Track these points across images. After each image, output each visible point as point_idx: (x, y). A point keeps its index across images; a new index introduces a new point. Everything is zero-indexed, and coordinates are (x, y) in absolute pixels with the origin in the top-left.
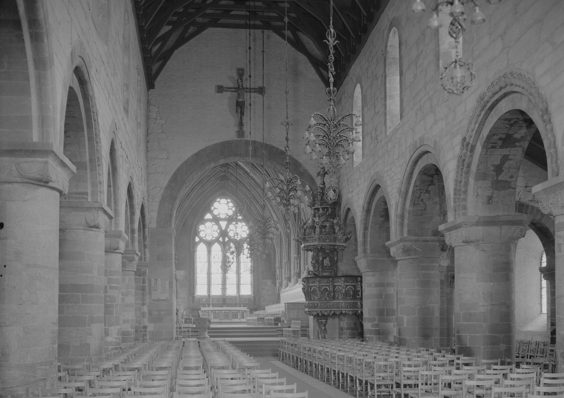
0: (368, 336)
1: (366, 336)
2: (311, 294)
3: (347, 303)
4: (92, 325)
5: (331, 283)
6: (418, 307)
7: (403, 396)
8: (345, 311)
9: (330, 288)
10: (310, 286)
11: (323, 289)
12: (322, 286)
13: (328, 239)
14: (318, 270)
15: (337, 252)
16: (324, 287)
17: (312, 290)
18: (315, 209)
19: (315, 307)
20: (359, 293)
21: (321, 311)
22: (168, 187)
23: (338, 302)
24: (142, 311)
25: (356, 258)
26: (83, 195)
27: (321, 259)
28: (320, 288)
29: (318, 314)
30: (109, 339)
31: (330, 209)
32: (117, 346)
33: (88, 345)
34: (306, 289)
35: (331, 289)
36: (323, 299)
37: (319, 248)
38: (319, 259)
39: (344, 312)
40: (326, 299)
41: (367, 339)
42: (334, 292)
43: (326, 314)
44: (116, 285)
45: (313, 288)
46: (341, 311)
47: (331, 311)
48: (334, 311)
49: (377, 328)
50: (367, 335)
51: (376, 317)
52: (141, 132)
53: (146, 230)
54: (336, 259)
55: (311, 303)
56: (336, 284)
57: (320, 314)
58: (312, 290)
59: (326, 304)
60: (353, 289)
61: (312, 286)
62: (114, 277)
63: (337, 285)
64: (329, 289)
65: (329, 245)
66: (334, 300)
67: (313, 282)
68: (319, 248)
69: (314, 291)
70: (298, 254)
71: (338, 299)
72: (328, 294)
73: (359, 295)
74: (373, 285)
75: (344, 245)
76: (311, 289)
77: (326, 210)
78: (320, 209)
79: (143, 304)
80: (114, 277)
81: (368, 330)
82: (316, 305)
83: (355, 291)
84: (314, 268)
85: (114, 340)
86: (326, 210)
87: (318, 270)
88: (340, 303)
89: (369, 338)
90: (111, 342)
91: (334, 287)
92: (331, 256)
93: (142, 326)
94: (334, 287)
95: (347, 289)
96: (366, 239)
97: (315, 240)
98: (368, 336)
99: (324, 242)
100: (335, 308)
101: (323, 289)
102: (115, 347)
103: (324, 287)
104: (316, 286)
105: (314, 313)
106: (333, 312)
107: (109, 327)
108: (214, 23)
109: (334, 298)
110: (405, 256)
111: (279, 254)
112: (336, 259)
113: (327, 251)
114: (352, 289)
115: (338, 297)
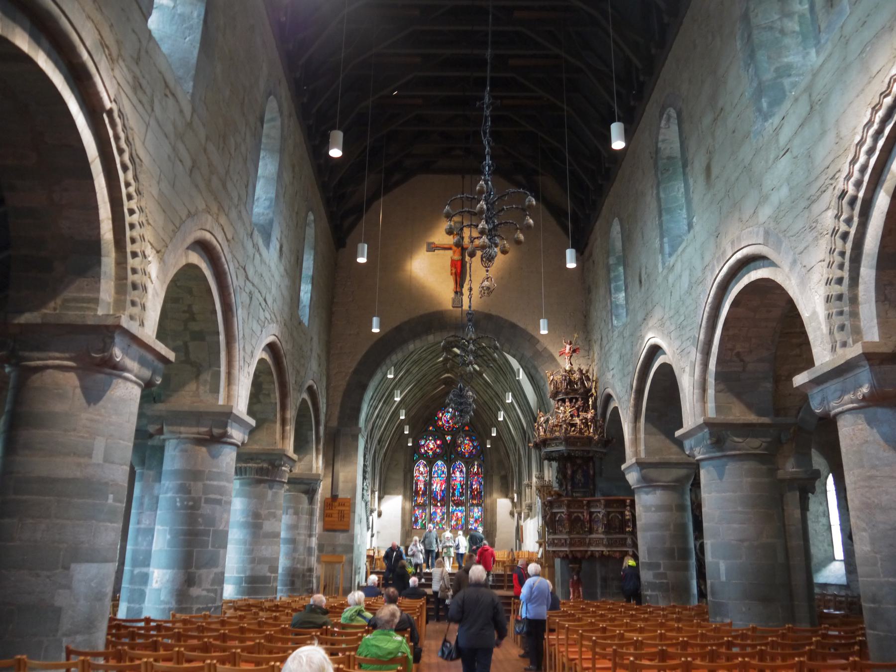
0: (649, 593)
1: (646, 593)
2: (557, 524)
3: (611, 539)
4: (73, 566)
5: (585, 507)
6: (746, 544)
8: (609, 551)
9: (584, 516)
10: (555, 513)
11: (573, 517)
12: (571, 512)
13: (580, 442)
14: (566, 488)
15: (594, 463)
17: (557, 518)
18: (558, 401)
19: (562, 545)
20: (629, 524)
21: (571, 551)
22: (356, 372)
24: (307, 546)
25: (623, 467)
26: (89, 302)
27: (569, 472)
28: (569, 515)
29: (567, 556)
30: (195, 591)
31: (580, 399)
32: (210, 605)
33: (58, 611)
34: (548, 517)
35: (585, 516)
37: (566, 455)
38: (567, 473)
39: (608, 553)
40: (578, 533)
41: (648, 598)
42: (591, 521)
43: (579, 555)
44: (219, 497)
45: (559, 515)
46: (602, 551)
47: (586, 551)
48: (592, 551)
49: (665, 581)
50: (647, 593)
51: (661, 562)
52: (279, 255)
53: (322, 428)
54: (591, 472)
55: (557, 539)
56: (593, 510)
57: (570, 556)
58: (557, 518)
61: (558, 513)
62: (215, 483)
63: (596, 512)
64: (582, 518)
65: (582, 450)
67: (560, 507)
68: (566, 455)
69: (561, 520)
70: (540, 471)
72: (581, 525)
73: (629, 527)
74: (653, 509)
75: (604, 451)
76: (555, 517)
77: (574, 401)
78: (567, 400)
79: (310, 536)
80: (215, 483)
81: (649, 583)
82: (563, 541)
84: (561, 485)
85: (204, 593)
86: (574, 401)
87: (566, 488)
89: (650, 596)
90: (198, 597)
91: (591, 514)
92: (585, 468)
93: (306, 567)
94: (591, 514)
95: (610, 517)
96: (638, 436)
97: (561, 443)
98: (649, 593)
101: (573, 517)
102: (205, 606)
103: (575, 514)
104: (563, 512)
105: (561, 554)
107: (195, 571)
108: (427, 167)
109: (591, 531)
110: (714, 452)
111: (517, 475)
112: (591, 472)
113: (579, 461)
114: (618, 517)
115: (597, 530)
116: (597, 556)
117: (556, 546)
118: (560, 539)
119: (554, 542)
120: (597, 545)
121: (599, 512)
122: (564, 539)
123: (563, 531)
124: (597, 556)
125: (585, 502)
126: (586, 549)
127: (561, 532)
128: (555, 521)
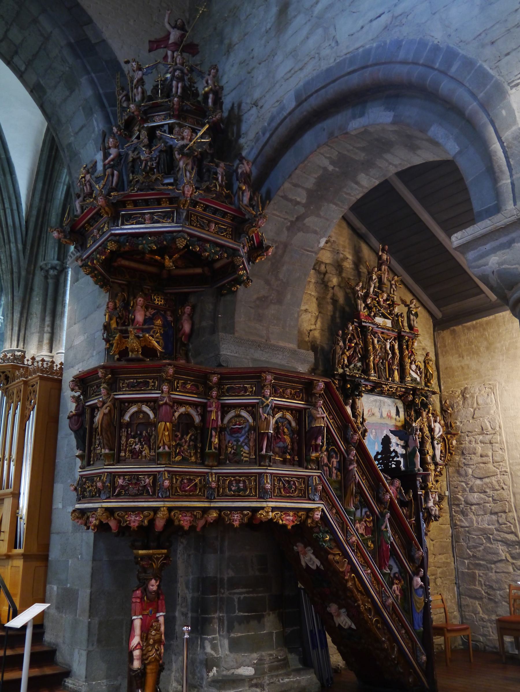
7: (9, 676)
11: (177, 414)
13: (216, 224)
16: (182, 410)
17: (127, 418)
23: (241, 475)
36: (178, 458)
37: (181, 244)
43: (185, 521)
45: (134, 409)
46: (255, 510)
47: (205, 510)
48: (220, 509)
54: (187, 327)
58: (127, 418)
59: (190, 481)
60: (294, 424)
64: (197, 419)
66: (220, 463)
71: (239, 462)
73: (317, 448)
76: (122, 414)
82: (148, 481)
83: (299, 433)
88: (248, 475)
99: (202, 227)
100: (223, 496)
101: (177, 414)
103: (182, 410)
106: (215, 514)
114: (290, 423)
116: (236, 524)
117: (119, 495)
118: (135, 477)
119: (113, 482)
120: (238, 495)
121: (245, 406)
122: (149, 474)
123: (146, 452)
124: (236, 524)
125: (215, 379)
126: (206, 505)
127: (136, 455)
128: (121, 425)
